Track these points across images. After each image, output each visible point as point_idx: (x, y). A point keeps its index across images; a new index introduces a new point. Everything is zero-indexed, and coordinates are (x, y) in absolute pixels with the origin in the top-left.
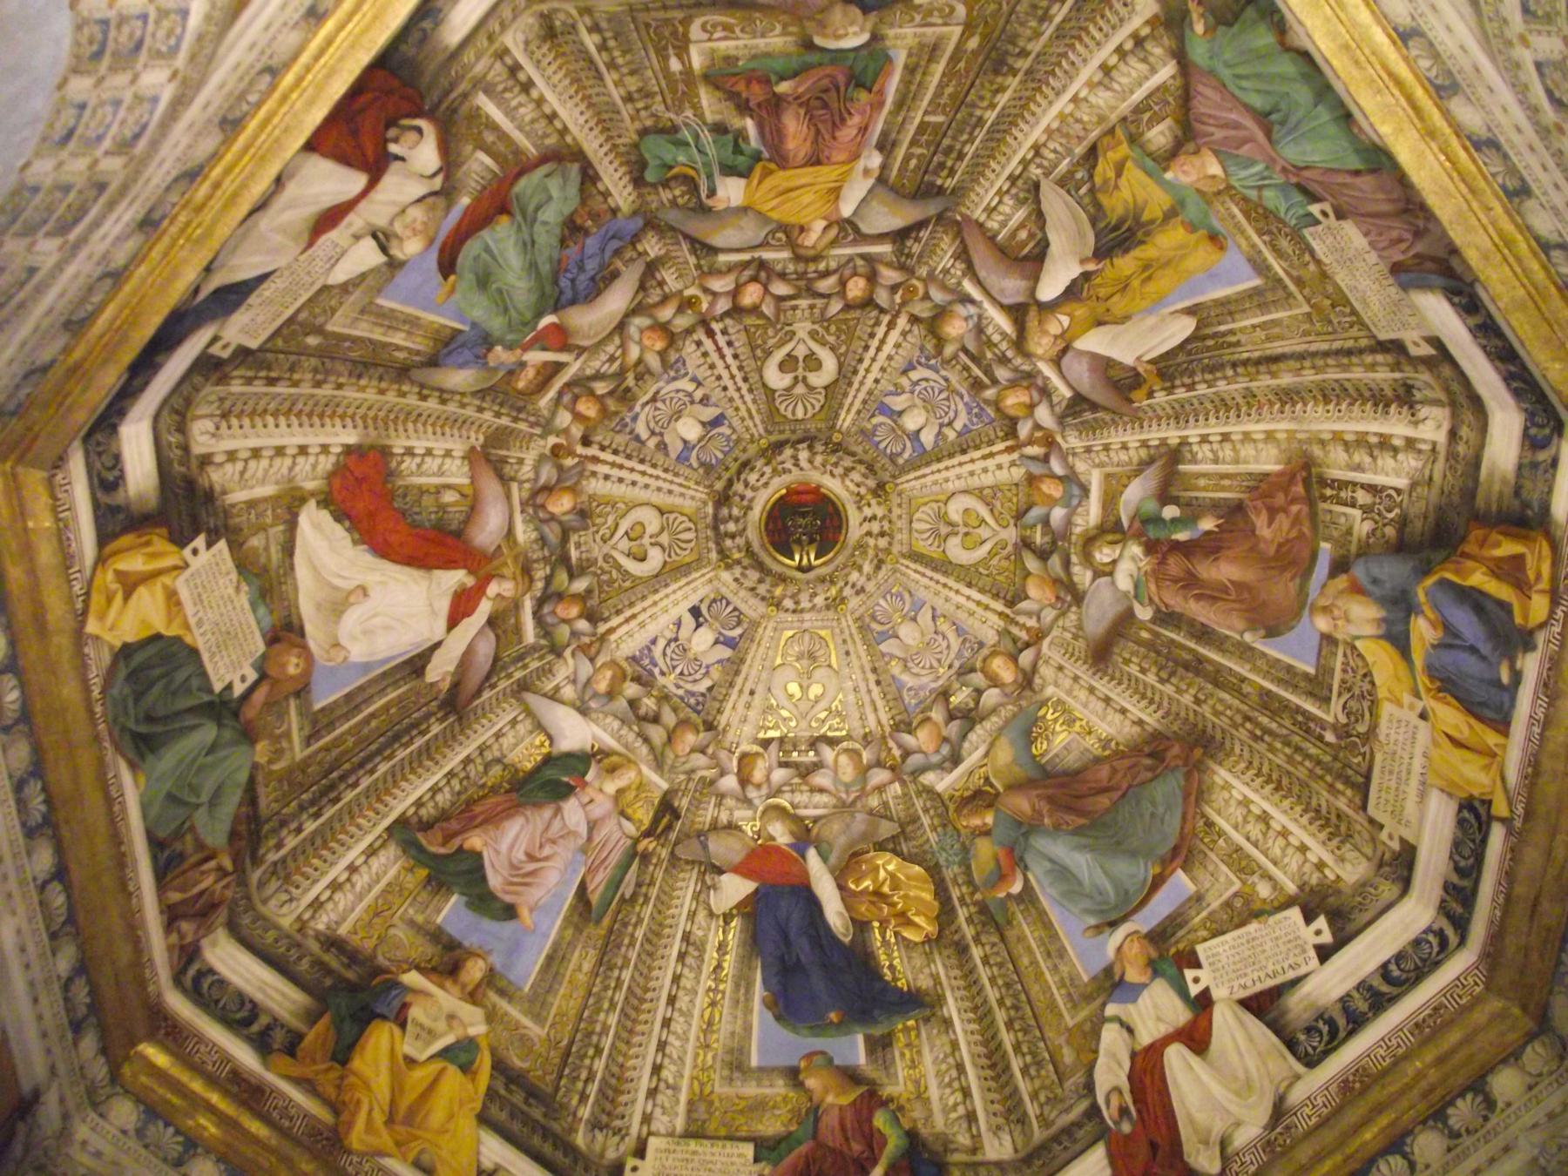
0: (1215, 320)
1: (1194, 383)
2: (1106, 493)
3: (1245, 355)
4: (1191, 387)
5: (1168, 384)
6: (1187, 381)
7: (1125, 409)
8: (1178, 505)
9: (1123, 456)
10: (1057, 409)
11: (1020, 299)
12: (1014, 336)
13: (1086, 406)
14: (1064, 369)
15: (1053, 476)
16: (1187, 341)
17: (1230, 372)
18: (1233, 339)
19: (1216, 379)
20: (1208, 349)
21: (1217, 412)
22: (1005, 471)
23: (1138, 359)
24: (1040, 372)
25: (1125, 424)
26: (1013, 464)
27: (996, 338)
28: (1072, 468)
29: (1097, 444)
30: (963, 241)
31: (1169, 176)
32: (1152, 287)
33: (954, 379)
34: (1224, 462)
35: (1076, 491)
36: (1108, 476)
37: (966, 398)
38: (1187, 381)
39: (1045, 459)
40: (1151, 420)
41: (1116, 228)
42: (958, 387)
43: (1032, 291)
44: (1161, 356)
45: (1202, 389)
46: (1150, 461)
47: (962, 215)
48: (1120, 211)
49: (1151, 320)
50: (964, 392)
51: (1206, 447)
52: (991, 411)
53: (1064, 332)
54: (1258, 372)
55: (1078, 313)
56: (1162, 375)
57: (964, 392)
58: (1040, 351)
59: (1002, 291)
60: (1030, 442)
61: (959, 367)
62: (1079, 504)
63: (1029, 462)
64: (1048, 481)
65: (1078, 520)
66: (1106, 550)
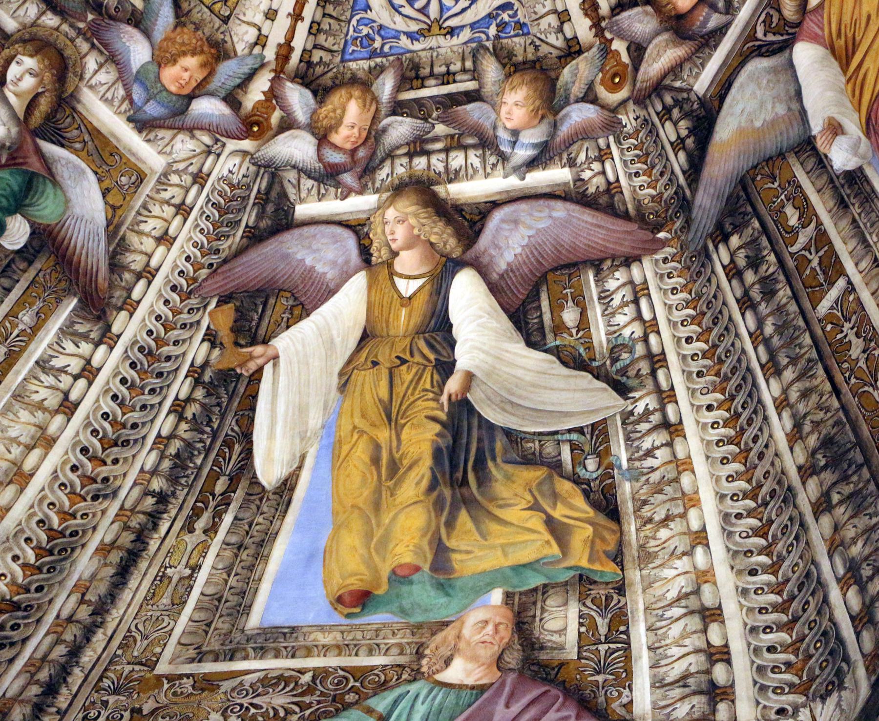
0: (246, 515)
1: (181, 418)
2: (114, 152)
3: (164, 527)
4: (178, 408)
5: (207, 378)
6: (192, 410)
7: (219, 283)
8: (18, 252)
9: (151, 225)
10: (292, 175)
11: (484, 241)
12: (440, 190)
13: (263, 224)
14: (339, 230)
15: (199, 90)
16: (248, 453)
17: (157, 484)
18: (201, 524)
19: (162, 457)
20: (214, 477)
21: (114, 423)
22: (259, 19)
23: (276, 358)
24: (361, 192)
25: (197, 267)
26: (261, 41)
27: (457, 160)
28: (191, 130)
29: (198, 198)
30: (626, 216)
31: (496, 596)
32: (361, 453)
33: (447, 46)
34: (32, 376)
35: (153, 109)
36: (141, 178)
37: (405, 42)
38: (192, 410)
39: (232, 100)
40: (176, 312)
41: (480, 465)
42: (432, 42)
43: (483, 271)
44: (255, 397)
45: (164, 423)
46: (115, 266)
47: (664, 243)
48: (501, 489)
49: (315, 420)
50: (417, 46)
51: (75, 366)
52: (360, 66)
53: (392, 274)
54: (126, 528)
55: (404, 312)
56: (227, 377)
57: (417, 46)
58: (391, 213)
59: (516, 222)
60: (273, 95)
61: (456, 67)
62: (129, 96)
63: (246, 69)
64: (199, 76)
65: (106, 76)
66: (28, 82)
